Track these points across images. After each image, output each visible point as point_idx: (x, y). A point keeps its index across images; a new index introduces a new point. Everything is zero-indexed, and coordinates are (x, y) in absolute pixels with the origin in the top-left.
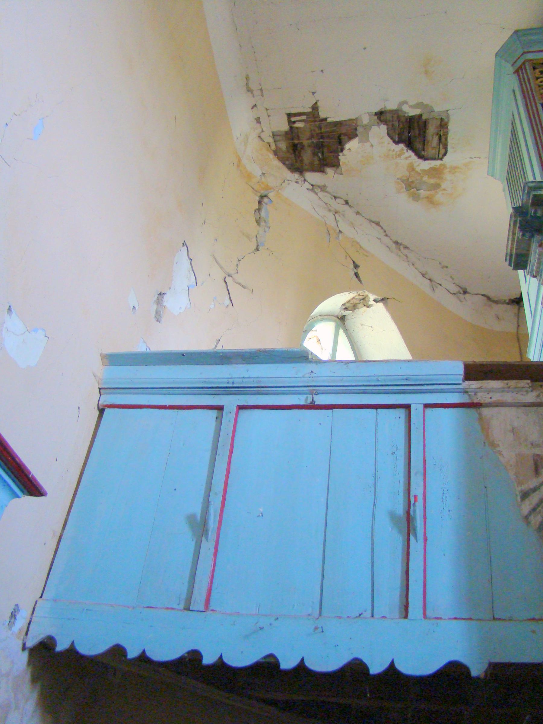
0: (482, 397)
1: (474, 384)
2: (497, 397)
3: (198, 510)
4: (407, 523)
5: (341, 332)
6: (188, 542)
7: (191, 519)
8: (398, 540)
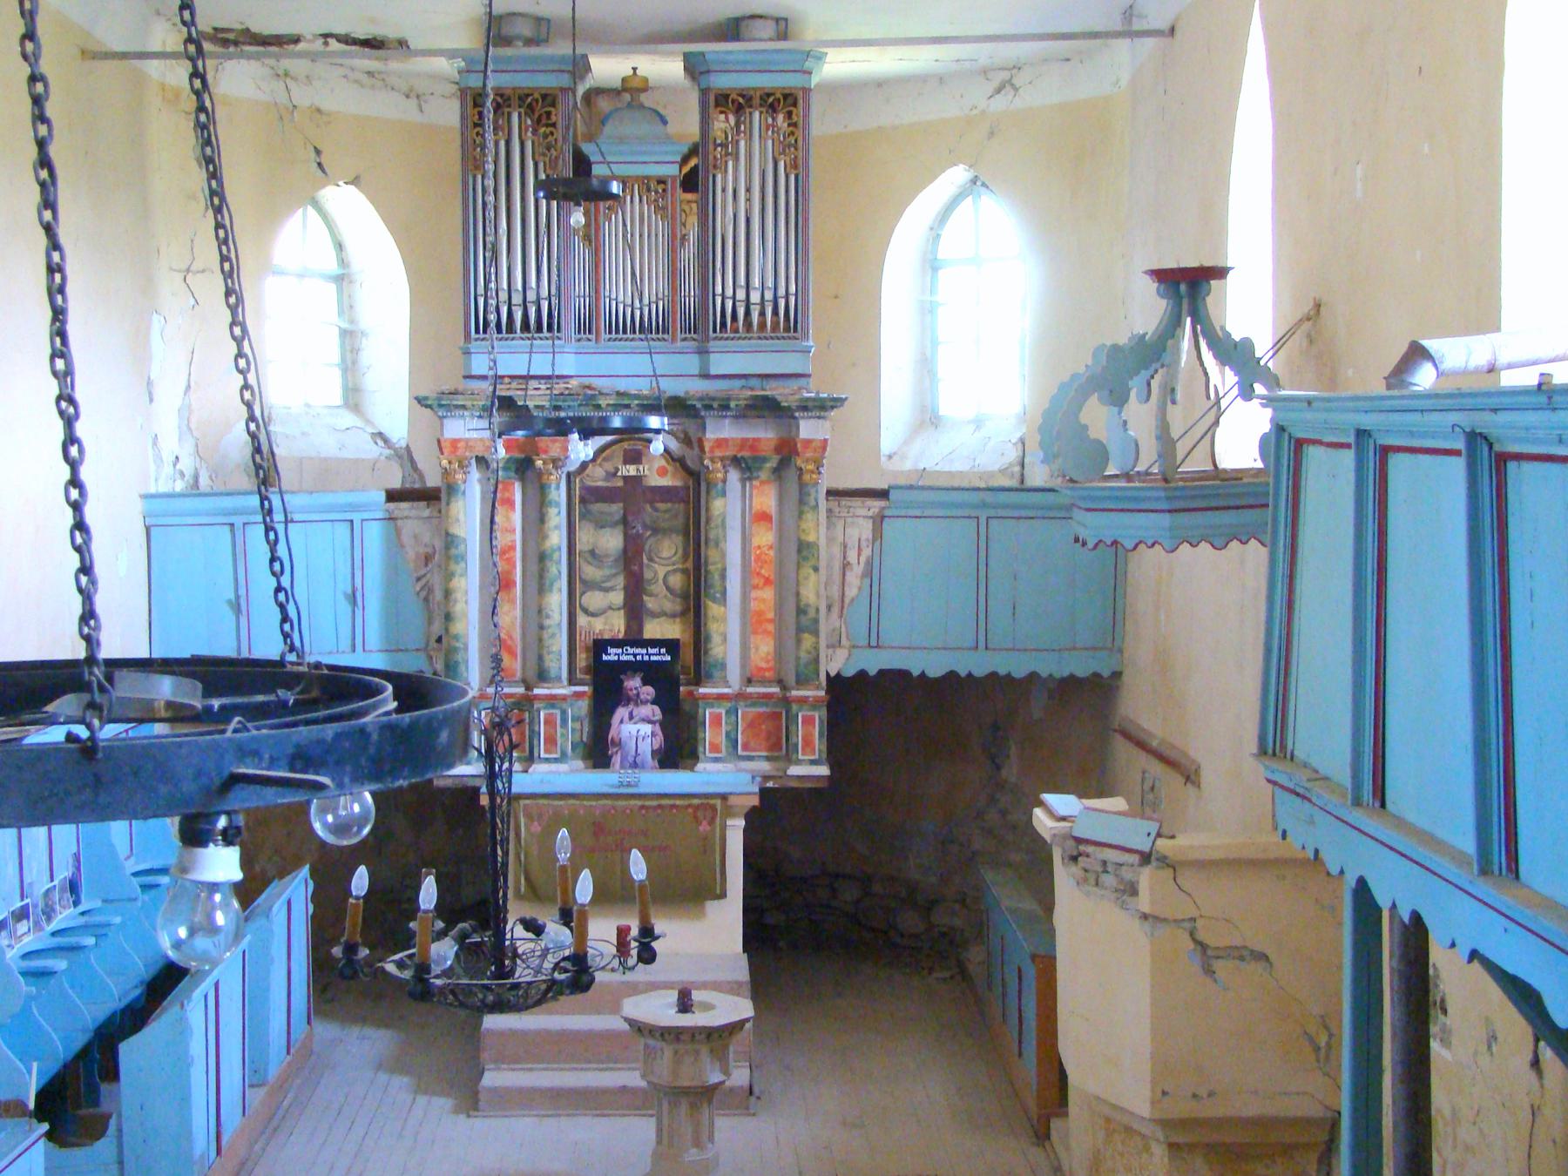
0: (397, 514)
1: (392, 505)
2: (406, 513)
3: (232, 596)
4: (353, 598)
5: (310, 210)
6: (229, 615)
7: (229, 602)
8: (350, 609)
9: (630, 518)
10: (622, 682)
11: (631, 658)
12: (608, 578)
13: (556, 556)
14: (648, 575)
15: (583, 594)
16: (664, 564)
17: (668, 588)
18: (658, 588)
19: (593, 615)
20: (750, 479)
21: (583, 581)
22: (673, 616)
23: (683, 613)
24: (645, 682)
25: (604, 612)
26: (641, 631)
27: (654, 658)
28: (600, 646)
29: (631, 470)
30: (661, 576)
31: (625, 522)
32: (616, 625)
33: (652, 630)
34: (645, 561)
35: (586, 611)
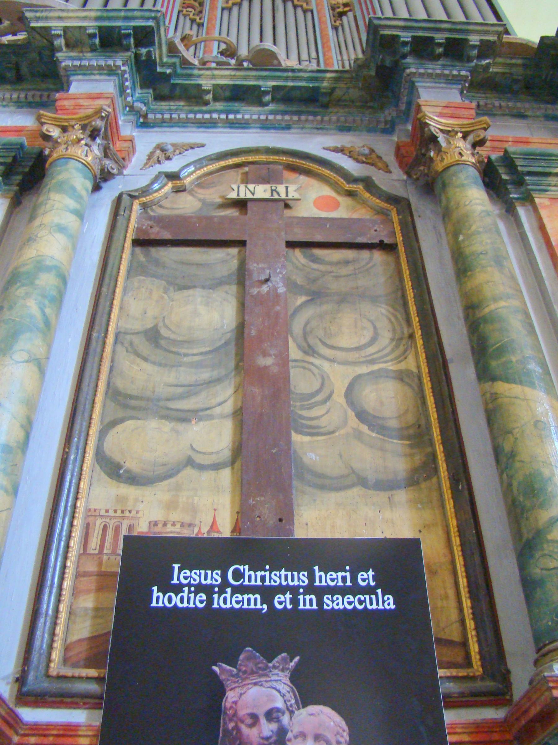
9: (253, 266)
10: (220, 691)
11: (253, 602)
12: (192, 390)
13: (47, 280)
14: (301, 382)
15: (109, 426)
16: (350, 364)
17: (362, 416)
18: (334, 413)
19: (133, 479)
20: (528, 199)
21: (113, 393)
22: (385, 485)
23: (412, 481)
24: (308, 691)
25: (169, 473)
26: (285, 517)
27: (335, 603)
28: (147, 559)
29: (261, 191)
30: (340, 386)
31: (242, 276)
32: (210, 507)
33: (317, 519)
34: (294, 353)
35: (114, 470)
